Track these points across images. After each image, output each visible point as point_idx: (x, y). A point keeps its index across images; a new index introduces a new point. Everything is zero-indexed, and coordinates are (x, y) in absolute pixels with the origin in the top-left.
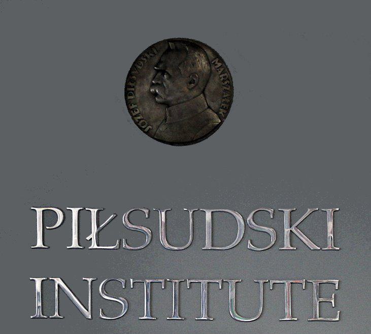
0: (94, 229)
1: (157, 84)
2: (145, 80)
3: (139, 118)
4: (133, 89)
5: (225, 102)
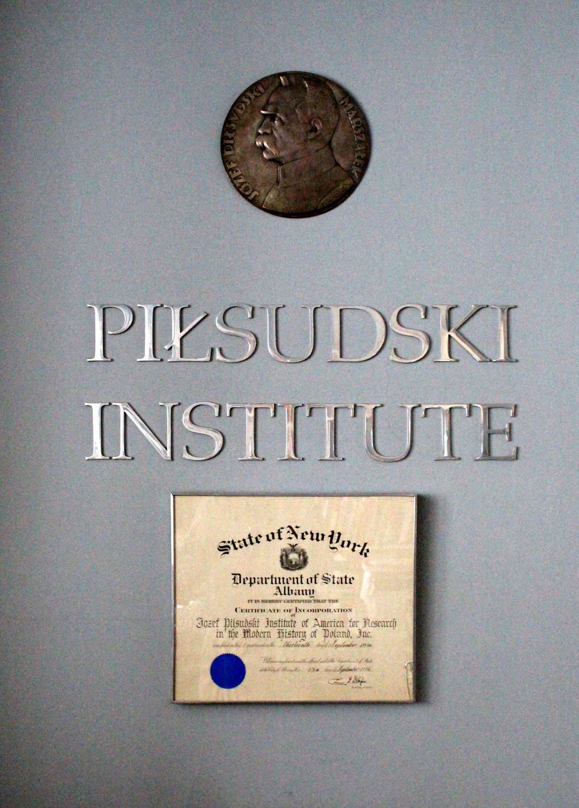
0: (176, 335)
1: (265, 134)
2: (248, 129)
3: (241, 181)
4: (232, 142)
5: (359, 157)
